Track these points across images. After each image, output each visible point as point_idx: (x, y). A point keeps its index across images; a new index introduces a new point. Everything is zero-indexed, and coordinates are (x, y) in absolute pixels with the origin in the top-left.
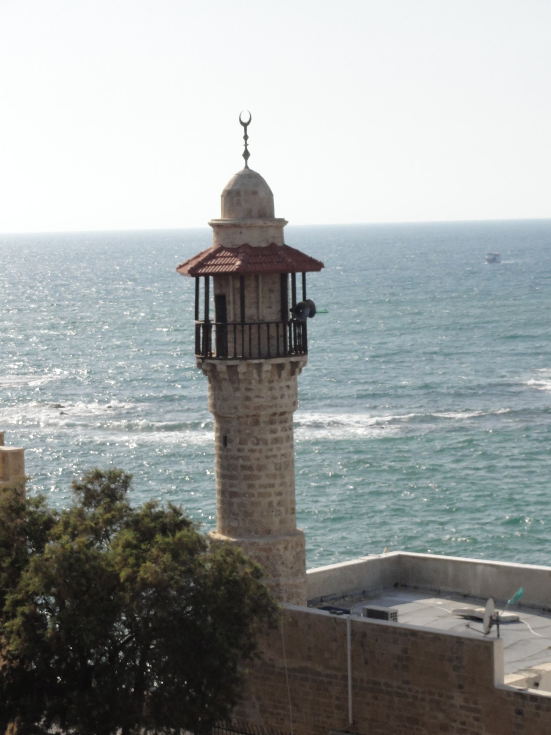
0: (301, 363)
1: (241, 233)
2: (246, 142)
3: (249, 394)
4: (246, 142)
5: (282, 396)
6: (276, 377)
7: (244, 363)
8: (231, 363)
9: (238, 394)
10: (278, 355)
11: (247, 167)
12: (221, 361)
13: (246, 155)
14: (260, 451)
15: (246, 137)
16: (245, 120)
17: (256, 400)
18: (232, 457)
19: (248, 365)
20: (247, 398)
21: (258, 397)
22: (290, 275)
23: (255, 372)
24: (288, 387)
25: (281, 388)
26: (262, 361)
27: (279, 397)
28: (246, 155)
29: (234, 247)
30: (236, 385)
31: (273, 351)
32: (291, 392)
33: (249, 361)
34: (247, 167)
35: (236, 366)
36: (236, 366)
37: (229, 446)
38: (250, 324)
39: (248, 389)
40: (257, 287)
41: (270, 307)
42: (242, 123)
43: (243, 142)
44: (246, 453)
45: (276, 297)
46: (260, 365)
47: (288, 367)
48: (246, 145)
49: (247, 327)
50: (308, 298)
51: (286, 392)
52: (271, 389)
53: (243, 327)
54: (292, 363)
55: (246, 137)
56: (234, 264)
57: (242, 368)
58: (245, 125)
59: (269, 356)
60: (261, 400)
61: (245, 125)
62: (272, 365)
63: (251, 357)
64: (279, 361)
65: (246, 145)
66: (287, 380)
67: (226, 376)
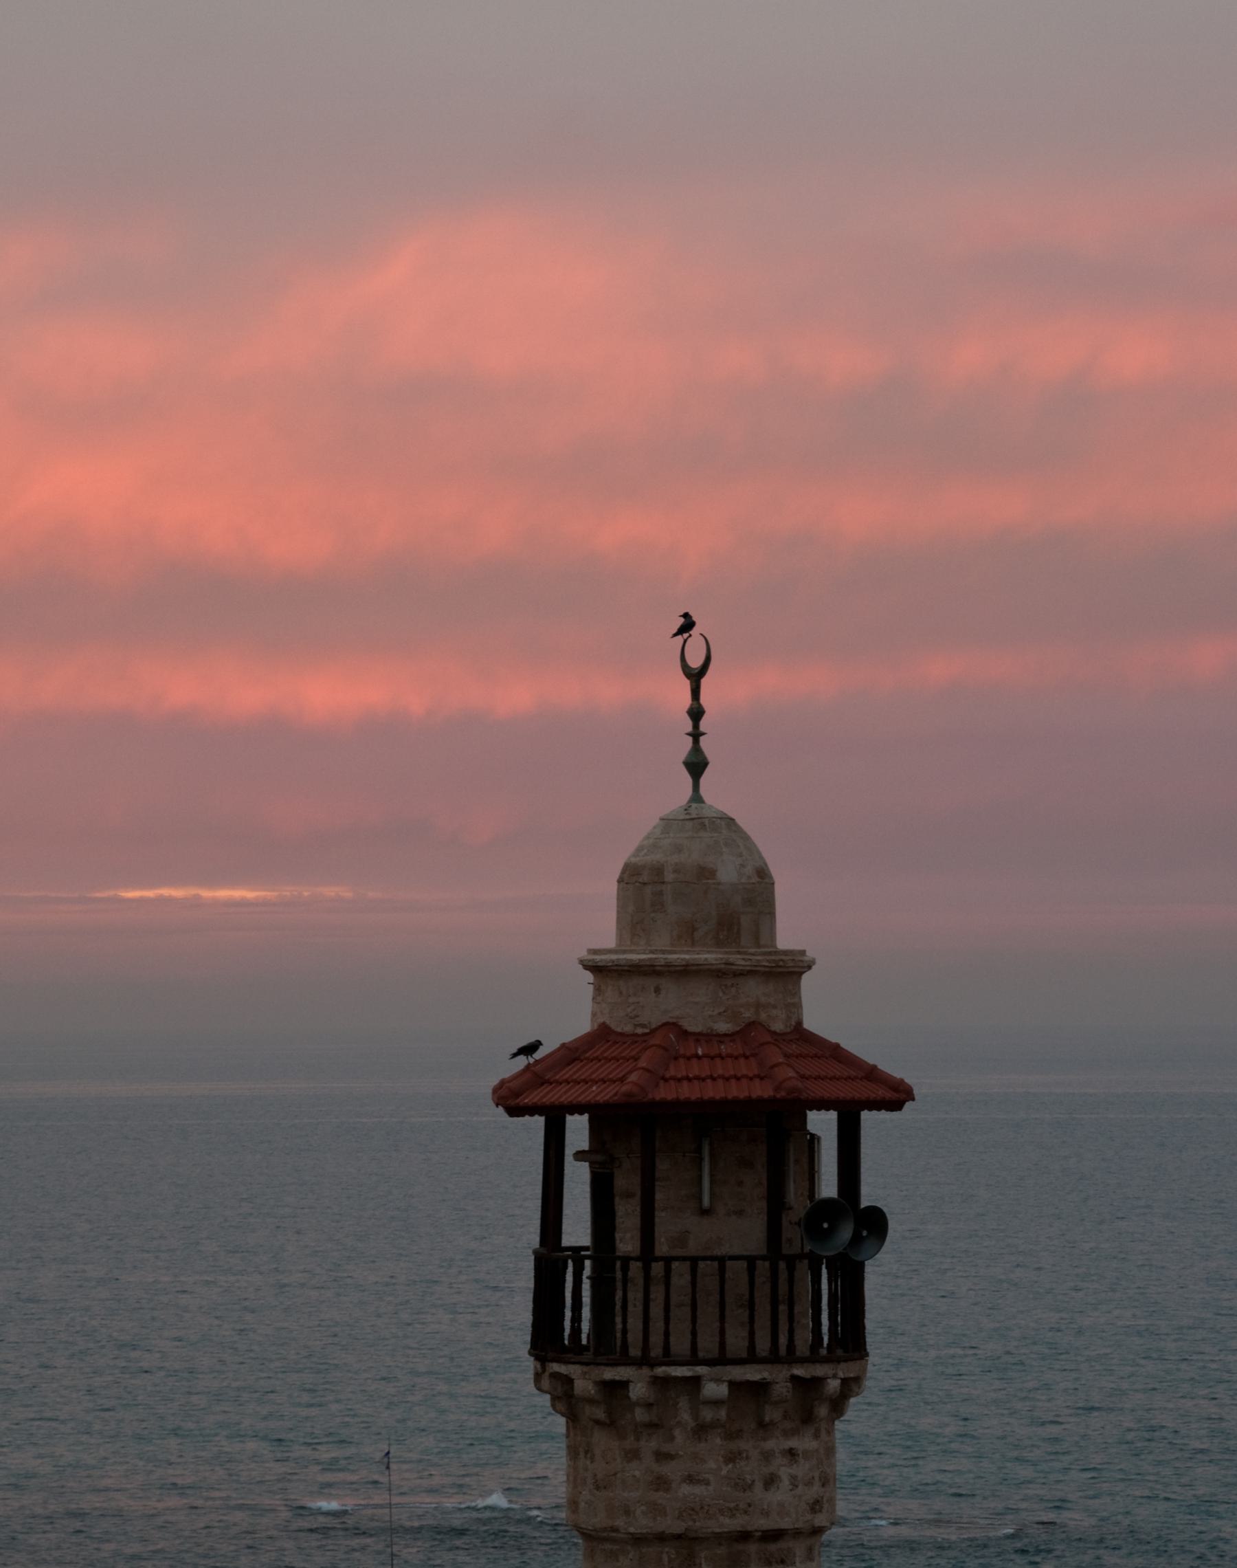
0: (833, 1385)
1: (657, 990)
2: (696, 725)
3: (667, 1469)
4: (696, 725)
5: (770, 1481)
7: (646, 1371)
8: (609, 1374)
9: (636, 1470)
10: (752, 1358)
12: (585, 1369)
13: (696, 766)
17: (686, 1489)
19: (657, 1381)
20: (661, 1483)
21: (690, 1479)
22: (823, 1123)
23: (684, 1403)
24: (791, 1453)
25: (767, 1456)
26: (701, 1370)
27: (759, 1486)
28: (696, 766)
29: (639, 1031)
31: (736, 1341)
32: (802, 1469)
33: (660, 1371)
35: (624, 1385)
36: (624, 1385)
38: (668, 1260)
39: (661, 1457)
40: (699, 1150)
41: (740, 1213)
46: (696, 1381)
47: (782, 1389)
48: (696, 735)
49: (657, 1268)
51: (784, 1473)
52: (731, 1458)
53: (647, 1270)
54: (794, 1378)
56: (622, 1080)
57: (638, 1391)
59: (722, 1359)
60: (699, 1490)
62: (733, 1385)
63: (668, 1358)
64: (752, 1373)
65: (696, 735)
66: (787, 1434)
67: (600, 1413)
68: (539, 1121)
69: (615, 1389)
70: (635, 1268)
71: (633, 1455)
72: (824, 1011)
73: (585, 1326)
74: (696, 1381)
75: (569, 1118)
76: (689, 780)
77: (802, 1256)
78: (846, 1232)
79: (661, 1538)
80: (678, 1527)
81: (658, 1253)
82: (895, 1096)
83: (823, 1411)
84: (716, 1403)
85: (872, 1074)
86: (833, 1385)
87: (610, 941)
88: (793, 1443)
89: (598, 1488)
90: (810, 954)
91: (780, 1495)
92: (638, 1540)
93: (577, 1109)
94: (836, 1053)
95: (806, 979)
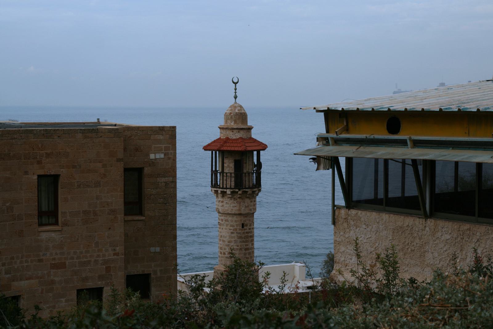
11: (236, 103)
13: (236, 97)
15: (236, 89)
16: (235, 81)
18: (247, 233)
28: (236, 97)
30: (251, 200)
34: (236, 103)
37: (245, 228)
42: (233, 82)
43: (234, 91)
48: (236, 93)
55: (236, 89)
58: (235, 83)
61: (235, 83)
65: (236, 93)
72: (255, 134)
73: (255, 182)
75: (261, 151)
76: (234, 99)
81: (224, 172)
82: (264, 147)
85: (260, 144)
87: (223, 124)
89: (246, 207)
90: (253, 126)
93: (255, 150)
94: (255, 141)
95: (252, 130)
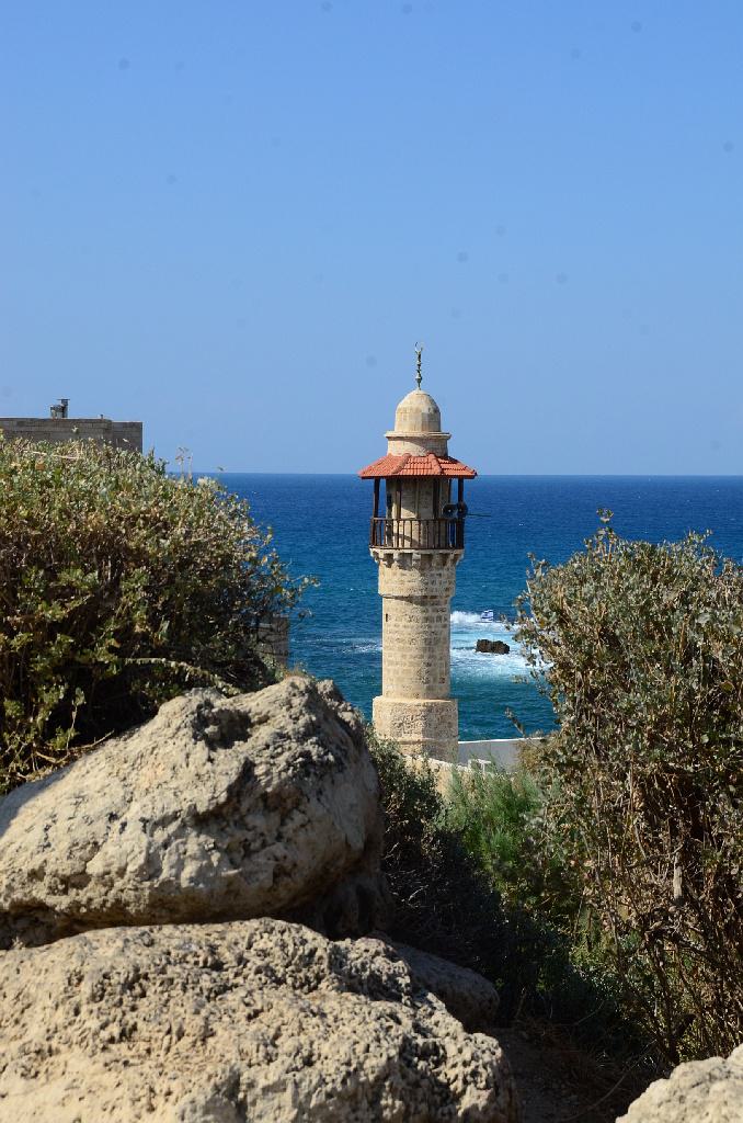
0: (452, 556)
6: (428, 566)
8: (388, 551)
14: (412, 627)
23: (409, 561)
24: (440, 575)
25: (432, 575)
32: (443, 579)
38: (404, 520)
40: (414, 492)
44: (401, 628)
45: (430, 499)
49: (401, 522)
50: (465, 500)
51: (438, 580)
57: (396, 556)
64: (428, 552)
66: (438, 569)
68: (373, 481)
69: (390, 556)
70: (395, 523)
71: (395, 574)
74: (411, 554)
77: (443, 519)
78: (456, 513)
79: (402, 598)
80: (406, 595)
83: (449, 564)
84: (417, 560)
86: (452, 556)
88: (440, 571)
91: (437, 586)
92: (396, 598)
